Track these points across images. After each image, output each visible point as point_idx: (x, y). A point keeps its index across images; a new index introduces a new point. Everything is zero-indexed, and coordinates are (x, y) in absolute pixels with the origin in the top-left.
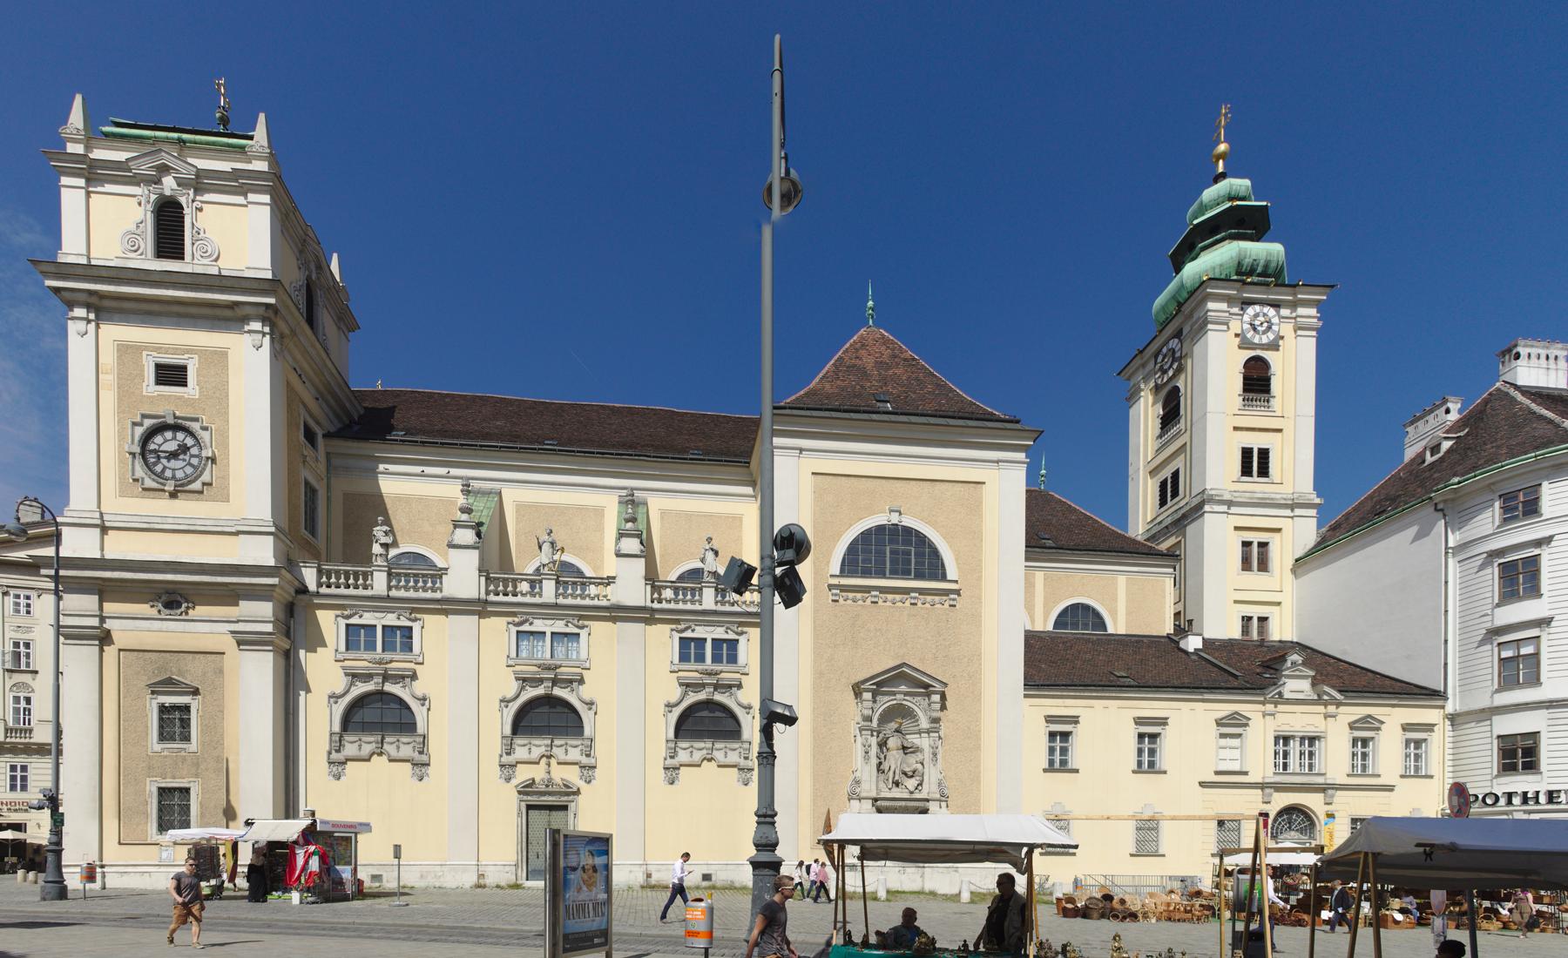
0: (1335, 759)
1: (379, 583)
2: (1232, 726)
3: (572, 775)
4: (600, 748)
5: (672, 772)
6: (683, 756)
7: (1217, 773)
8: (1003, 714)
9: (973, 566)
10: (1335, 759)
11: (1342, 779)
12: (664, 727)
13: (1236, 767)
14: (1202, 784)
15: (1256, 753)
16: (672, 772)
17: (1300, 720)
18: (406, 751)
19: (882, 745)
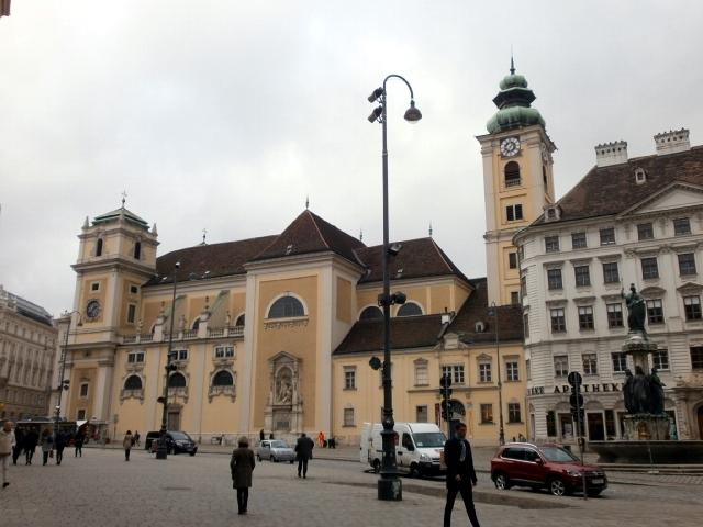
0: (472, 376)
1: (138, 340)
2: (421, 364)
3: (180, 401)
4: (190, 390)
5: (211, 398)
6: (214, 392)
7: (417, 386)
8: (324, 369)
9: (314, 311)
10: (472, 376)
11: (474, 385)
12: (209, 381)
13: (425, 382)
14: (409, 392)
15: (433, 378)
16: (211, 398)
17: (452, 359)
18: (139, 395)
19: (278, 383)
